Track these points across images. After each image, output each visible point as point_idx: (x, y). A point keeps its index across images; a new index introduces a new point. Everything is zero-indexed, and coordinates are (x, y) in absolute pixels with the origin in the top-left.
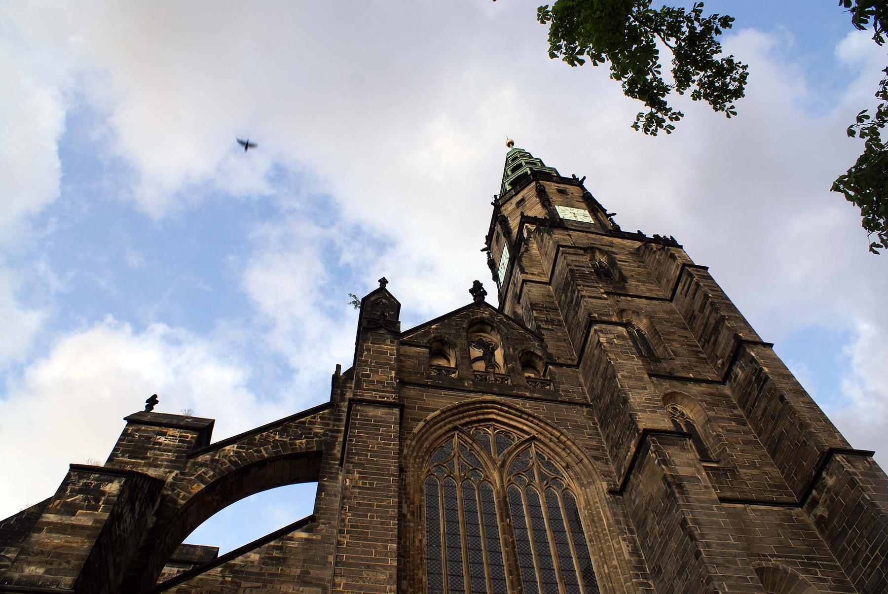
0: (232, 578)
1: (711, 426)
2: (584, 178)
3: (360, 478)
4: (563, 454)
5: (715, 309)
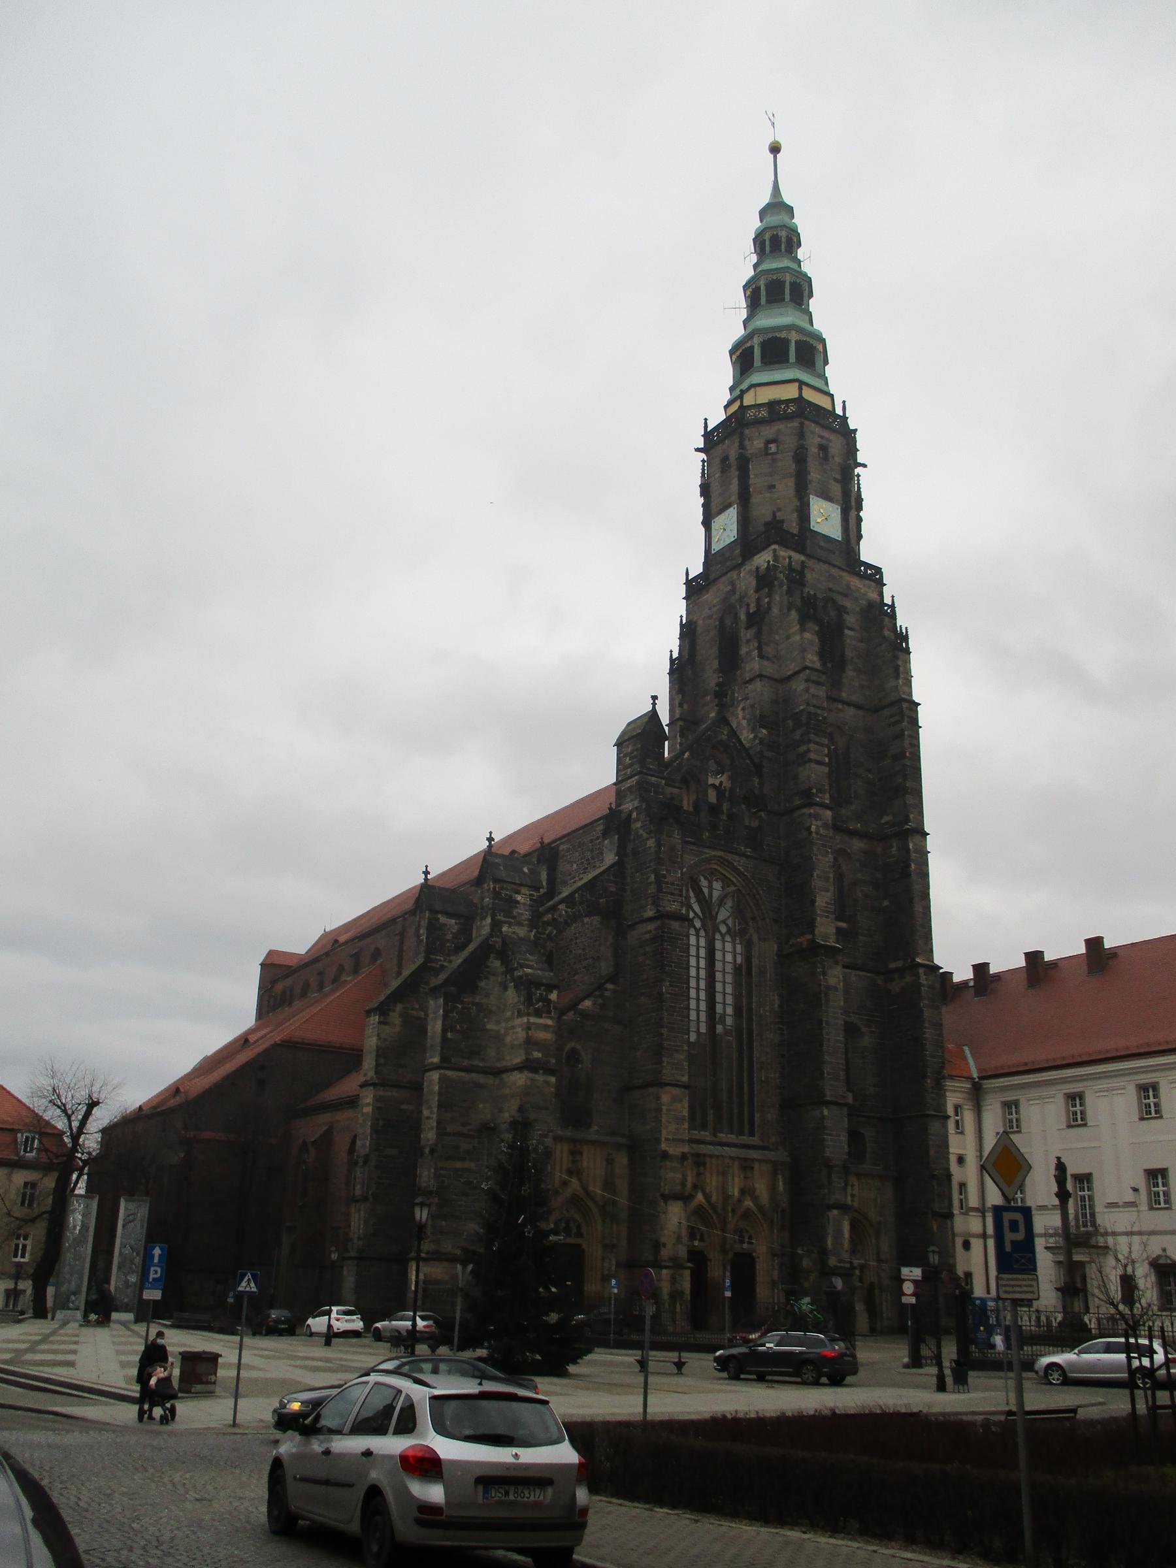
3: (671, 986)
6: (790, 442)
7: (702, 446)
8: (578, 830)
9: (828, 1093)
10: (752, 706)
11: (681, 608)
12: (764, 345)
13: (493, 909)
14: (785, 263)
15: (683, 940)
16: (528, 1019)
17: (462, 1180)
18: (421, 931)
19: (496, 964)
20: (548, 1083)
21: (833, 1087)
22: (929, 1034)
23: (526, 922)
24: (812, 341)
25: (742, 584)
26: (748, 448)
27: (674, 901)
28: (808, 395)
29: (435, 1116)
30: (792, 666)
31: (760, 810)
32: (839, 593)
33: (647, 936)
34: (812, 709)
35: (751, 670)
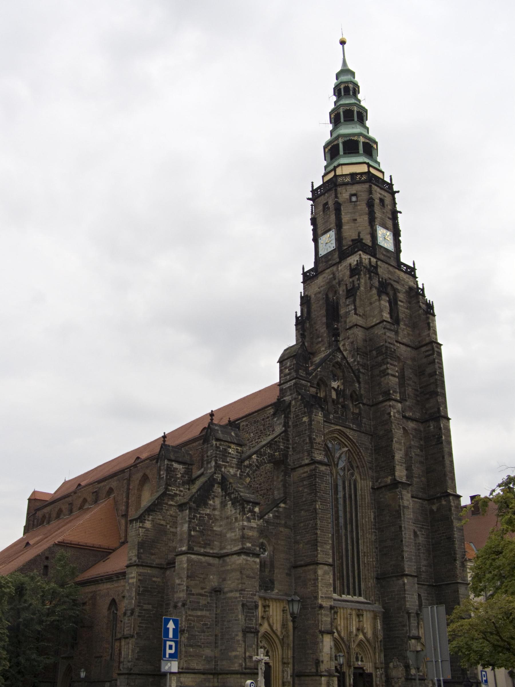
0: (267, 524)
1: (411, 451)
2: (398, 192)
3: (321, 504)
4: (357, 460)
5: (437, 386)
6: (364, 196)
7: (310, 196)
8: (253, 413)
9: (406, 569)
10: (352, 343)
11: (300, 288)
12: (344, 143)
13: (216, 457)
14: (353, 101)
15: (326, 477)
16: (243, 523)
17: (202, 623)
18: (162, 473)
19: (217, 489)
20: (255, 562)
21: (409, 567)
22: (457, 535)
23: (235, 465)
24: (371, 143)
25: (340, 274)
26: (340, 198)
27: (320, 454)
28: (372, 171)
29: (185, 584)
30: (375, 320)
31: (359, 403)
32: (394, 281)
33: (305, 475)
34: (387, 344)
35: (350, 322)
